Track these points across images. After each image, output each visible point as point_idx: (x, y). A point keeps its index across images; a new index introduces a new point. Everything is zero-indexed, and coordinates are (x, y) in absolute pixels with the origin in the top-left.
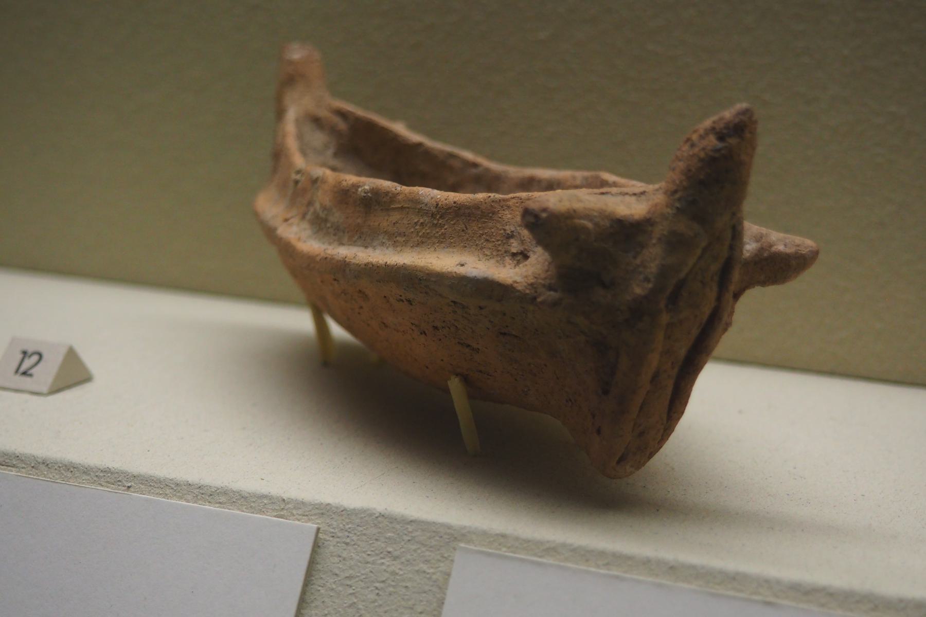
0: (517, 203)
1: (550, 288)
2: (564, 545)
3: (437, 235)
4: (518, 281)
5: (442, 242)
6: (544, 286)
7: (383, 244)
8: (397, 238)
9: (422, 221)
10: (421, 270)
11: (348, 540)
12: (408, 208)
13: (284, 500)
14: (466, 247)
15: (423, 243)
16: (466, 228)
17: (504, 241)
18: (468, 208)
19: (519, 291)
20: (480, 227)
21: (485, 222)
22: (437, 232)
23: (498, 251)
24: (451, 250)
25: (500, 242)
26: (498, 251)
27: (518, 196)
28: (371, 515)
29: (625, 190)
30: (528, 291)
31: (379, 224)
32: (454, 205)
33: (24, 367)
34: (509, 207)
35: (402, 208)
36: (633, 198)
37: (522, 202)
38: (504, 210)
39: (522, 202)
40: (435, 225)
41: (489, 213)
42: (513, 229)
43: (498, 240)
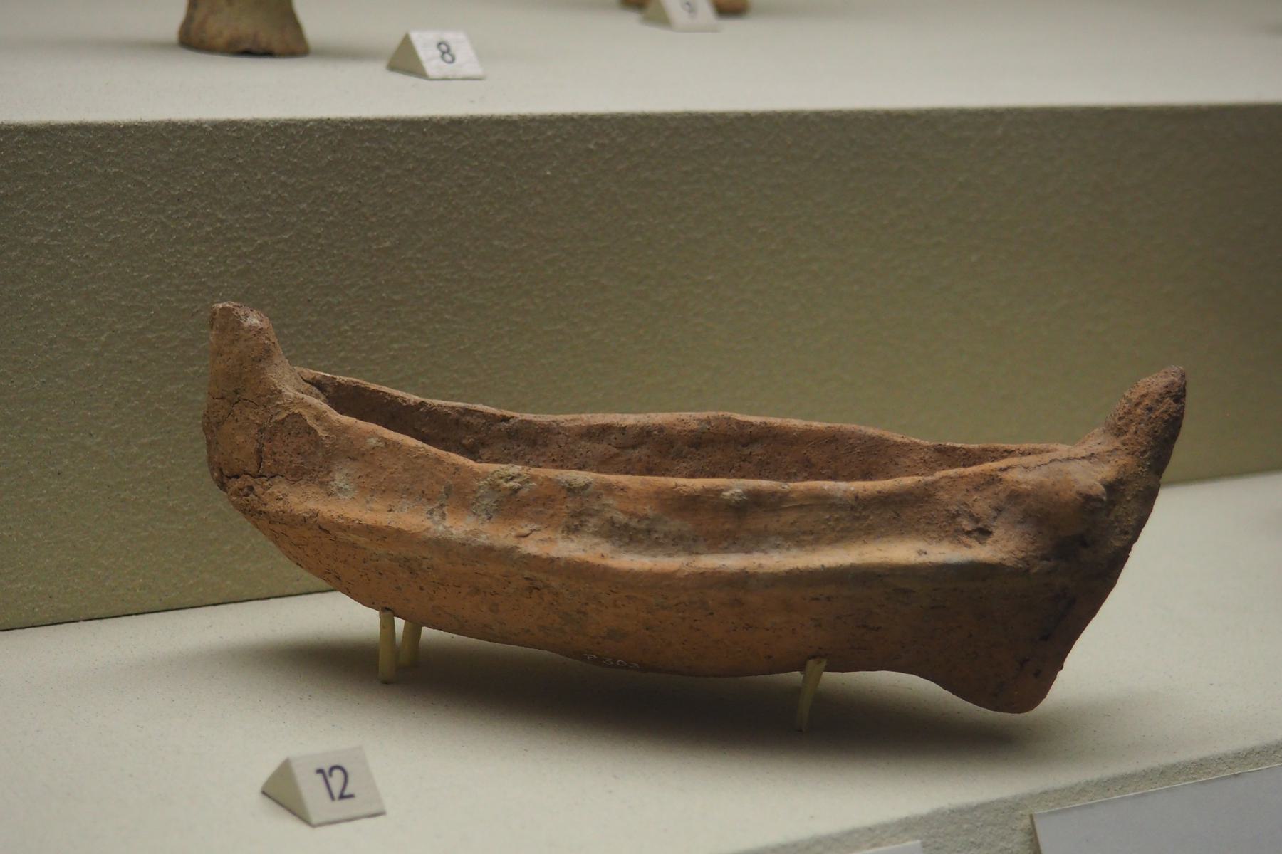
0: (949, 482)
1: (1043, 558)
2: (1088, 783)
6: (1036, 557)
7: (777, 546)
11: (937, 845)
13: (870, 829)
14: (903, 533)
15: (842, 537)
16: (898, 515)
17: (950, 521)
19: (1008, 567)
21: (921, 506)
23: (946, 531)
25: (945, 523)
27: (945, 475)
28: (943, 814)
29: (1053, 455)
30: (1020, 566)
31: (766, 526)
33: (336, 790)
34: (942, 487)
35: (801, 506)
36: (1085, 462)
37: (954, 481)
40: (858, 519)
42: (956, 508)
43: (942, 522)
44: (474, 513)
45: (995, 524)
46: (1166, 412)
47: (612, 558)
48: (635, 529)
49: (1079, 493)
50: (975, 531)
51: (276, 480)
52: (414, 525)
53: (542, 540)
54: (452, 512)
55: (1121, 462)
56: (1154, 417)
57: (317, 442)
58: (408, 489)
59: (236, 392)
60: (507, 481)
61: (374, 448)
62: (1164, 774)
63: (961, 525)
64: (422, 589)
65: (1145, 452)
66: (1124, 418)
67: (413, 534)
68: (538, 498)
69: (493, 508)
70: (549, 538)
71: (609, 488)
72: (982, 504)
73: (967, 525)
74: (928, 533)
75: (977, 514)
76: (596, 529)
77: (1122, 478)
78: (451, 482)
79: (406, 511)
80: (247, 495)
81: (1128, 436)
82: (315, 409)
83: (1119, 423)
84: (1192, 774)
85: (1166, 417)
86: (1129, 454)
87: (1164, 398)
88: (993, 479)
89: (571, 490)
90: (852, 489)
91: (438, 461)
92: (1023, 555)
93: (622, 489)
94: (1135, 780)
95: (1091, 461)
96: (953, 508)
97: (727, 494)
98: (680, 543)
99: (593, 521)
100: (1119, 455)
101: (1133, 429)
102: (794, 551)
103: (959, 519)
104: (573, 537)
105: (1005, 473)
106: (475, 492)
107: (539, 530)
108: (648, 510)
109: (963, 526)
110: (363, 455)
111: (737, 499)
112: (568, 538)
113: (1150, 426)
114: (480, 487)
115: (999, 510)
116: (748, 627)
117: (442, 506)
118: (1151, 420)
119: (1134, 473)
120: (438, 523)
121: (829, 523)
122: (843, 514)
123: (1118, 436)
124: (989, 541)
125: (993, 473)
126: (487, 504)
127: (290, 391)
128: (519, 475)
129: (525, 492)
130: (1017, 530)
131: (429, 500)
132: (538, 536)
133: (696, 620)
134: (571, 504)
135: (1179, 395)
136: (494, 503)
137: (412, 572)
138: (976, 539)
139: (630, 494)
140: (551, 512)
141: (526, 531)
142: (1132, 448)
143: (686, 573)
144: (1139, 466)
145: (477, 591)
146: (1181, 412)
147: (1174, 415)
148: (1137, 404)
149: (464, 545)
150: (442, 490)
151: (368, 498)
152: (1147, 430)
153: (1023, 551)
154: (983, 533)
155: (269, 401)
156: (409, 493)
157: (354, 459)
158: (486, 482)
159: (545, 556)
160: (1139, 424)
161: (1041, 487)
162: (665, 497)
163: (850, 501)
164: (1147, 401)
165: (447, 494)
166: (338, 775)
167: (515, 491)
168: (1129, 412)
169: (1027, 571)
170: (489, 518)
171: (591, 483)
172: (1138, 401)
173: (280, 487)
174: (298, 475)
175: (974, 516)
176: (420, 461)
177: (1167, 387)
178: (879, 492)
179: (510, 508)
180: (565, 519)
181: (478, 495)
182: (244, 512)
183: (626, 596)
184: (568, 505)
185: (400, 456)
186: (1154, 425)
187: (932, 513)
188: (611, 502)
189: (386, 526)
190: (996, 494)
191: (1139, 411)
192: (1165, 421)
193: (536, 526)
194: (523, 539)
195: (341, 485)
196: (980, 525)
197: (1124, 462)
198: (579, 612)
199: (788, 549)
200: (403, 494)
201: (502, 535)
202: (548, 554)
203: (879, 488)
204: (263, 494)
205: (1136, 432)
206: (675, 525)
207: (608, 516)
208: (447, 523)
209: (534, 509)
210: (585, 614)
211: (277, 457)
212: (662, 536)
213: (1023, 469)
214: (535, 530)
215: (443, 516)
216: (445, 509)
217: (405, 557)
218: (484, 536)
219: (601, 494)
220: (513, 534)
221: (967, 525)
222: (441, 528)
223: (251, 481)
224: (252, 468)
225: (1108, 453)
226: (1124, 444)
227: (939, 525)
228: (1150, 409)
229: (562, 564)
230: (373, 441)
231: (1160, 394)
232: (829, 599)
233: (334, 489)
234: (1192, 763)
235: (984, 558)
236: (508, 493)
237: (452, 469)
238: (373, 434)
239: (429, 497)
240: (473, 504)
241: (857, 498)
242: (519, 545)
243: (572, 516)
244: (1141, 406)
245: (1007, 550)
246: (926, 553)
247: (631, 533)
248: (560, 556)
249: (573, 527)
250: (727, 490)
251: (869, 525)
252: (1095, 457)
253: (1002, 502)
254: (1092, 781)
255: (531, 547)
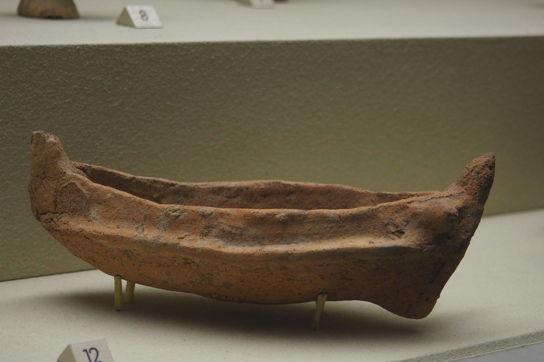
0: (383, 209)
1: (429, 244)
2: (452, 351)
3: (342, 231)
4: (411, 244)
5: (346, 234)
6: (426, 244)
7: (302, 241)
8: (314, 236)
9: (330, 226)
10: (351, 249)
12: (318, 221)
14: (362, 234)
15: (333, 236)
16: (360, 225)
17: (384, 228)
18: (360, 215)
19: (413, 248)
20: (368, 223)
21: (370, 221)
22: (342, 230)
23: (382, 232)
24: (354, 236)
25: (382, 228)
26: (382, 232)
29: (433, 196)
30: (418, 248)
31: (297, 231)
32: (350, 215)
36: (448, 198)
38: (379, 213)
39: (386, 208)
40: (340, 227)
41: (372, 216)
42: (388, 221)
44: (158, 228)
45: (406, 228)
46: (486, 174)
47: (224, 247)
48: (234, 233)
49: (445, 213)
50: (397, 232)
51: (64, 214)
52: (129, 234)
53: (190, 240)
54: (147, 228)
55: (464, 198)
56: (480, 176)
57: (83, 196)
58: (126, 217)
59: (44, 173)
60: (173, 212)
61: (110, 198)
62: (487, 346)
63: (390, 229)
64: (134, 265)
65: (476, 193)
66: (466, 177)
67: (129, 238)
68: (188, 220)
69: (167, 225)
70: (194, 239)
71: (222, 215)
72: (399, 219)
73: (393, 229)
74: (374, 233)
75: (397, 224)
76: (216, 234)
77: (466, 206)
78: (147, 213)
79: (125, 228)
80: (50, 222)
81: (468, 186)
82: (82, 180)
83: (464, 180)
84: (501, 346)
85: (486, 177)
86: (469, 194)
87: (485, 168)
88: (404, 207)
89: (204, 216)
90: (338, 213)
91: (141, 203)
92: (419, 242)
93: (228, 215)
94: (475, 349)
95: (451, 198)
96: (386, 221)
97: (278, 216)
98: (257, 240)
99: (215, 230)
100: (464, 195)
101: (470, 182)
102: (310, 243)
103: (388, 227)
104: (205, 238)
105: (410, 204)
106: (158, 218)
107: (189, 235)
108: (241, 224)
109: (391, 230)
110: (105, 201)
111: (283, 218)
112: (202, 239)
113: (478, 181)
114: (160, 215)
115: (407, 222)
116: (289, 279)
117: (142, 225)
118: (479, 178)
119: (471, 203)
120: (140, 233)
121: (327, 229)
122: (334, 225)
123: (463, 186)
124: (403, 236)
125: (405, 204)
126: (164, 224)
127: (69, 172)
128: (179, 209)
129: (181, 217)
130: (416, 231)
131: (136, 222)
132: (188, 238)
133: (264, 277)
134: (204, 223)
135: (492, 167)
136: (167, 223)
137: (129, 256)
138: (397, 235)
139: (232, 218)
140: (194, 226)
141: (183, 236)
142: (470, 191)
143: (259, 254)
144: (473, 200)
145: (160, 265)
146: (493, 174)
147: (490, 175)
148: (472, 171)
149: (153, 243)
150: (143, 218)
151: (107, 222)
152: (477, 183)
153: (419, 241)
154: (400, 233)
155: (60, 177)
156: (126, 219)
157: (100, 204)
158: (163, 213)
159: (192, 247)
160: (473, 180)
161: (427, 210)
162: (248, 218)
163: (337, 219)
164: (477, 169)
165: (145, 219)
166: (94, 352)
167: (177, 217)
168: (469, 175)
169: (422, 250)
170: (165, 230)
171: (213, 212)
172: (472, 169)
173: (65, 218)
174: (73, 212)
175: (395, 225)
176: (132, 204)
177: (486, 162)
178: (350, 214)
179: (175, 225)
180: (201, 230)
181: (159, 219)
182: (48, 230)
183: (231, 266)
184: (202, 223)
185: (122, 202)
186: (480, 180)
187: (376, 224)
188: (223, 221)
189: (116, 235)
190: (406, 214)
191: (473, 174)
192: (485, 179)
193: (187, 234)
194: (181, 240)
195: (94, 216)
196: (399, 229)
197: (466, 198)
198: (209, 274)
199: (307, 242)
200: (124, 220)
201: (171, 238)
202: (193, 246)
203: (350, 212)
204: (58, 221)
205: (472, 184)
206: (253, 231)
207: (222, 227)
208: (145, 233)
209: (186, 225)
210: (212, 275)
211: (64, 204)
212: (247, 237)
213: (418, 202)
214: (187, 235)
215: (143, 230)
216: (144, 226)
217: (125, 250)
218: (163, 239)
219: (218, 218)
220: (177, 237)
221: (393, 229)
222: (142, 235)
223: (51, 215)
224: (52, 209)
225: (459, 194)
226: (466, 190)
227: (379, 229)
228: (478, 173)
229: (200, 251)
230: (109, 195)
231: (483, 166)
232: (327, 265)
233: (91, 218)
234: (502, 341)
235: (401, 244)
236: (174, 218)
237: (147, 207)
238: (109, 192)
239: (136, 221)
240: (157, 224)
241: (340, 217)
242: (180, 243)
243: (204, 228)
244: (474, 172)
245: (411, 240)
246: (373, 243)
247: (233, 236)
248: (199, 247)
249: (205, 233)
250: (278, 214)
251: (346, 230)
252: (453, 196)
253: (409, 218)
254: (454, 350)
255: (185, 243)
